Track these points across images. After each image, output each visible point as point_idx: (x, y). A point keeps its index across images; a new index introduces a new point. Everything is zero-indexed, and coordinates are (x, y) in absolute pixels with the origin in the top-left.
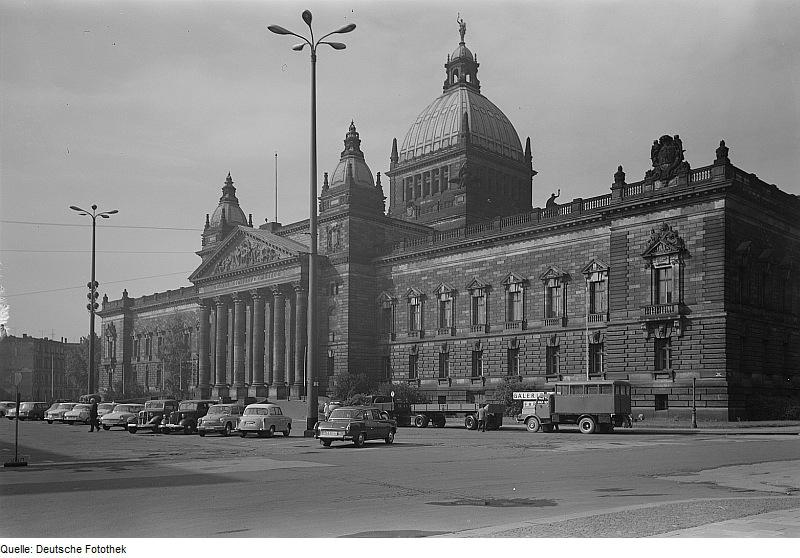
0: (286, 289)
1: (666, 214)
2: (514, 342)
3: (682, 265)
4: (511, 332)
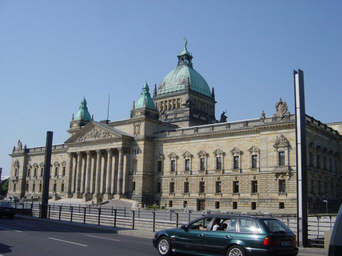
0: (115, 152)
1: (284, 131)
2: (219, 179)
3: (289, 151)
4: (217, 174)
